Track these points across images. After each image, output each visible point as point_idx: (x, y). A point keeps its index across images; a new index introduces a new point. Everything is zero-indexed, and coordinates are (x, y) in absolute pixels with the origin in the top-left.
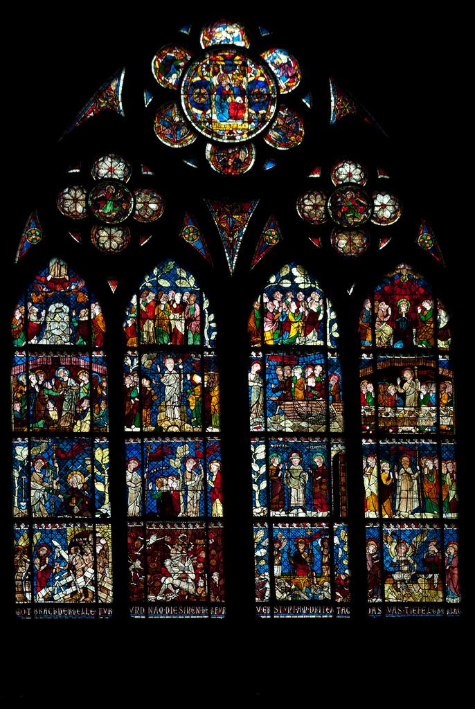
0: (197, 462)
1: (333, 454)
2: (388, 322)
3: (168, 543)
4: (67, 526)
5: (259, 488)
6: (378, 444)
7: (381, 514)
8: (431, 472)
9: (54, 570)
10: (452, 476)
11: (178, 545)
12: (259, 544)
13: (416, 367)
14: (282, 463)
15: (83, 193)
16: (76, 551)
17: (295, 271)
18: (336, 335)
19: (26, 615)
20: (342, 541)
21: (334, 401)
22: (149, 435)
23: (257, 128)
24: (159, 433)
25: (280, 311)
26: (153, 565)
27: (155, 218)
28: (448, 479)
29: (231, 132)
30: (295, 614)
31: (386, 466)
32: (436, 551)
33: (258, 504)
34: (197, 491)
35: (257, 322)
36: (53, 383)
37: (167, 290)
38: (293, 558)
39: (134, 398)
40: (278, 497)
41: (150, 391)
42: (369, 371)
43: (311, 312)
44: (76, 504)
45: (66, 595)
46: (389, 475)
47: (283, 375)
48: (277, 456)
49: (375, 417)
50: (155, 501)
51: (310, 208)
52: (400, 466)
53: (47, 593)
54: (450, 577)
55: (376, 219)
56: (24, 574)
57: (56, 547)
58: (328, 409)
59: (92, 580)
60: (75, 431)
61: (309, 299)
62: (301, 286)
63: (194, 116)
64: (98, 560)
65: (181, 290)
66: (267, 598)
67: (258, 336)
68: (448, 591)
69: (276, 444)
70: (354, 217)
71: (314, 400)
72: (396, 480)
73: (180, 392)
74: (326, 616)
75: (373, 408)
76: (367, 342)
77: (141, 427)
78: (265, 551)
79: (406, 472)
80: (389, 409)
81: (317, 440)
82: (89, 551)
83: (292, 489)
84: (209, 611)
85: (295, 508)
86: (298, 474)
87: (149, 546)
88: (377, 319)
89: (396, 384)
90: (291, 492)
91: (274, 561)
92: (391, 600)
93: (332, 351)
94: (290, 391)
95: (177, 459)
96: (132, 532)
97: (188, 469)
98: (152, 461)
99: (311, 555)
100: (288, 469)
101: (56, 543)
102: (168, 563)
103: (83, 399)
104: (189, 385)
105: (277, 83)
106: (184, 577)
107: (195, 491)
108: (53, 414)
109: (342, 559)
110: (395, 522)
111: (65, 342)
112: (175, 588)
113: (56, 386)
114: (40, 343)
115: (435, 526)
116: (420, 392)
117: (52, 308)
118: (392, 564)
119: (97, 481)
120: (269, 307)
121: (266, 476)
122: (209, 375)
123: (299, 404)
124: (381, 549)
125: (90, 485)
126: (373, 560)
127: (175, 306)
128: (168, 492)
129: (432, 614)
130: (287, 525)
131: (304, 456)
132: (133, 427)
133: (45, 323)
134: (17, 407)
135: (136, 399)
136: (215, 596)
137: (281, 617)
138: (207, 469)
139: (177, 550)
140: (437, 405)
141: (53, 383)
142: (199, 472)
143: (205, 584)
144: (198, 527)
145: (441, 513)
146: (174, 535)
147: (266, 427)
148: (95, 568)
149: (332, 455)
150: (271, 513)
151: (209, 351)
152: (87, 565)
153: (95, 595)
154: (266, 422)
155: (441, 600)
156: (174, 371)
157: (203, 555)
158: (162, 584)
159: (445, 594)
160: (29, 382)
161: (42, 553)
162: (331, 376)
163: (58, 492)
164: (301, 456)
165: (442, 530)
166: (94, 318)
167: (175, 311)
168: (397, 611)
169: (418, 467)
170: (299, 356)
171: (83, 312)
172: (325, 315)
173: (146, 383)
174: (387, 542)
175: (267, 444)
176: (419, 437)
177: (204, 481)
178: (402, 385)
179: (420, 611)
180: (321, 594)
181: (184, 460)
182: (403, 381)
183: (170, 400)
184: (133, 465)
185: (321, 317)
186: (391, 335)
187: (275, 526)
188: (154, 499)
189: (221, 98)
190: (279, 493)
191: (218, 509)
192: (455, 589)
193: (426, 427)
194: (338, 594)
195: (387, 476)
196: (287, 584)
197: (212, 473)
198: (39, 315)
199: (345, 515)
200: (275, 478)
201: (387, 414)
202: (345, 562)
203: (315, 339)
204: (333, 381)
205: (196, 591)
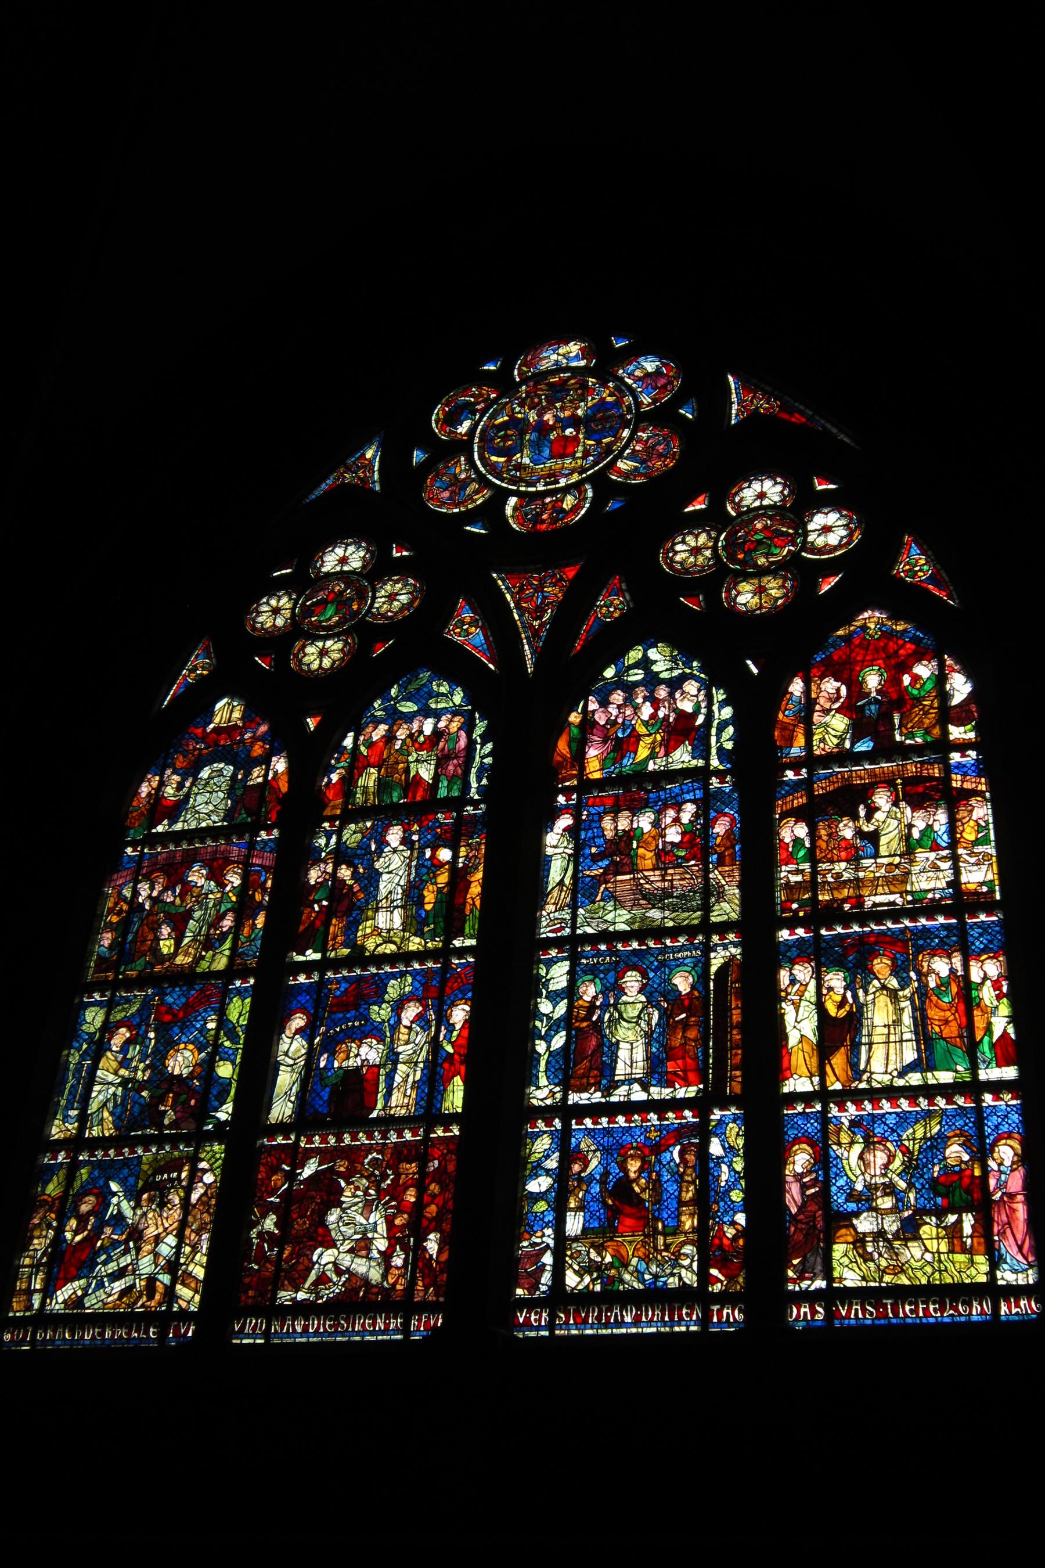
0: (426, 1007)
1: (716, 963)
2: (838, 711)
3: (340, 1175)
4: (144, 1151)
5: (549, 1047)
6: (818, 936)
7: (823, 1082)
8: (943, 984)
9: (99, 1244)
10: (996, 985)
11: (362, 1176)
12: (539, 1165)
13: (899, 781)
14: (601, 992)
15: (290, 599)
16: (151, 1200)
17: (653, 654)
18: (729, 745)
19: (23, 1341)
20: (731, 1147)
21: (721, 863)
22: (337, 964)
23: (596, 463)
24: (359, 957)
25: (620, 720)
26: (301, 1224)
27: (407, 613)
28: (987, 994)
29: (549, 476)
30: (607, 1325)
31: (836, 980)
32: (966, 1157)
33: (543, 1081)
34: (416, 1063)
35: (574, 745)
36: (178, 891)
37: (409, 718)
38: (612, 1194)
39: (319, 902)
40: (586, 1063)
41: (351, 886)
42: (800, 800)
43: (681, 714)
44: (172, 1107)
45: (110, 1295)
46: (844, 996)
47: (616, 828)
48: (592, 981)
49: (813, 885)
50: (328, 1090)
51: (684, 555)
52: (869, 973)
53: (75, 1292)
54: (1004, 1218)
55: (814, 550)
56: (39, 1253)
57: (114, 1194)
58: (706, 879)
59: (169, 1262)
60: (199, 970)
61: (677, 695)
62: (665, 675)
63: (493, 468)
64: (190, 1219)
65: (437, 715)
66: (543, 1288)
67: (573, 767)
68: (1001, 1256)
69: (593, 957)
70: (767, 555)
71: (679, 866)
72: (861, 1007)
73: (409, 881)
74: (683, 1329)
75: (806, 866)
76: (796, 750)
77: (324, 950)
78: (550, 1180)
79: (884, 987)
80: (843, 865)
81: (682, 940)
82: (177, 1201)
83: (622, 1045)
84: (406, 1324)
85: (623, 1082)
86: (636, 1013)
87: (301, 1182)
88: (817, 707)
89: (855, 817)
90: (618, 1048)
91: (567, 1201)
92: (849, 1284)
93: (720, 774)
94: (628, 855)
95: (384, 1006)
96: (270, 1155)
97: (406, 1022)
98: (334, 1013)
99: (656, 1186)
100: (615, 1006)
101: (114, 1187)
102: (333, 1217)
103: (225, 914)
104: (426, 867)
105: (635, 398)
106: (362, 1247)
107: (412, 1063)
108: (166, 946)
109: (729, 1189)
110: (857, 1097)
111: (214, 822)
112: (339, 1272)
113: (182, 896)
114: (179, 826)
115: (961, 1101)
116: (910, 826)
117: (205, 773)
118: (852, 1195)
119: (221, 1059)
120: (601, 719)
121: (567, 1022)
122: (469, 845)
123: (646, 877)
124: (823, 1160)
125: (207, 1068)
126: (804, 1187)
127: (422, 739)
128: (358, 1069)
129: (960, 1315)
130: (604, 1120)
131: (651, 975)
132: (309, 952)
133: (187, 796)
134: (106, 939)
135: (325, 903)
136: (426, 1288)
137: (574, 1332)
138: (443, 1018)
139: (357, 1188)
140: (953, 844)
141: (178, 891)
142: (425, 1025)
143: (406, 1260)
144: (408, 1136)
145: (974, 1068)
146: (354, 1155)
147: (574, 927)
148: (180, 1236)
149: (713, 969)
150: (570, 1097)
151: (475, 804)
152: (165, 1229)
153: (170, 1294)
154: (574, 916)
155: (983, 1279)
156: (401, 848)
157: (411, 1196)
158: (314, 1264)
159: (995, 1263)
160: (136, 893)
161: (84, 1208)
162: (716, 819)
163: (142, 1085)
164: (644, 975)
165: (979, 1110)
166: (273, 778)
167: (421, 747)
168: (864, 1310)
169: (912, 974)
170: (650, 791)
171: (256, 772)
172: (710, 716)
173: (345, 873)
174: (839, 1144)
175: (574, 959)
176: (913, 914)
177: (435, 1044)
178: (869, 817)
179: (926, 1311)
180: (672, 1275)
181: (398, 1007)
182: (872, 810)
183: (386, 897)
184: (298, 1021)
185: (700, 720)
186: (846, 732)
187: (577, 1124)
188: (326, 1086)
189: (540, 435)
190: (591, 1055)
191: (455, 1098)
192: (1020, 1248)
193: (929, 891)
194: (714, 1272)
195: (839, 998)
196: (593, 1254)
197: (453, 1025)
198: (180, 786)
199: (738, 1089)
200: (585, 1024)
201: (839, 875)
202: (736, 1196)
203: (687, 757)
204: (720, 828)
205: (384, 1276)
